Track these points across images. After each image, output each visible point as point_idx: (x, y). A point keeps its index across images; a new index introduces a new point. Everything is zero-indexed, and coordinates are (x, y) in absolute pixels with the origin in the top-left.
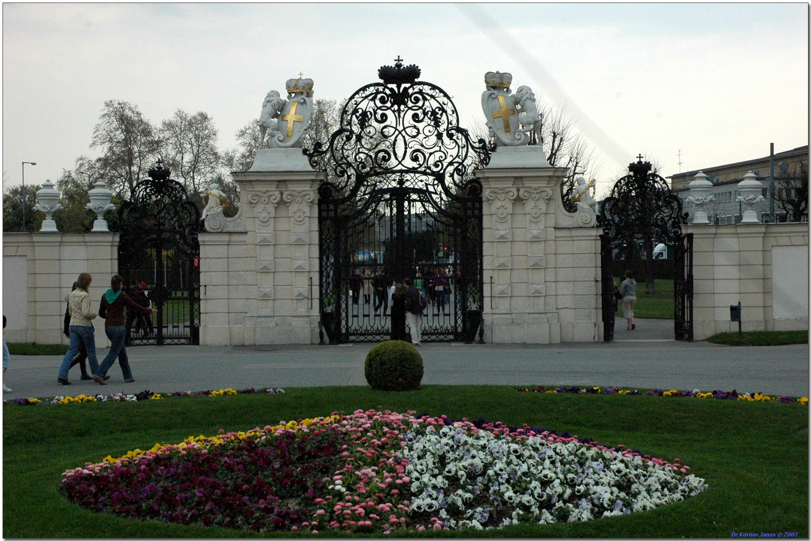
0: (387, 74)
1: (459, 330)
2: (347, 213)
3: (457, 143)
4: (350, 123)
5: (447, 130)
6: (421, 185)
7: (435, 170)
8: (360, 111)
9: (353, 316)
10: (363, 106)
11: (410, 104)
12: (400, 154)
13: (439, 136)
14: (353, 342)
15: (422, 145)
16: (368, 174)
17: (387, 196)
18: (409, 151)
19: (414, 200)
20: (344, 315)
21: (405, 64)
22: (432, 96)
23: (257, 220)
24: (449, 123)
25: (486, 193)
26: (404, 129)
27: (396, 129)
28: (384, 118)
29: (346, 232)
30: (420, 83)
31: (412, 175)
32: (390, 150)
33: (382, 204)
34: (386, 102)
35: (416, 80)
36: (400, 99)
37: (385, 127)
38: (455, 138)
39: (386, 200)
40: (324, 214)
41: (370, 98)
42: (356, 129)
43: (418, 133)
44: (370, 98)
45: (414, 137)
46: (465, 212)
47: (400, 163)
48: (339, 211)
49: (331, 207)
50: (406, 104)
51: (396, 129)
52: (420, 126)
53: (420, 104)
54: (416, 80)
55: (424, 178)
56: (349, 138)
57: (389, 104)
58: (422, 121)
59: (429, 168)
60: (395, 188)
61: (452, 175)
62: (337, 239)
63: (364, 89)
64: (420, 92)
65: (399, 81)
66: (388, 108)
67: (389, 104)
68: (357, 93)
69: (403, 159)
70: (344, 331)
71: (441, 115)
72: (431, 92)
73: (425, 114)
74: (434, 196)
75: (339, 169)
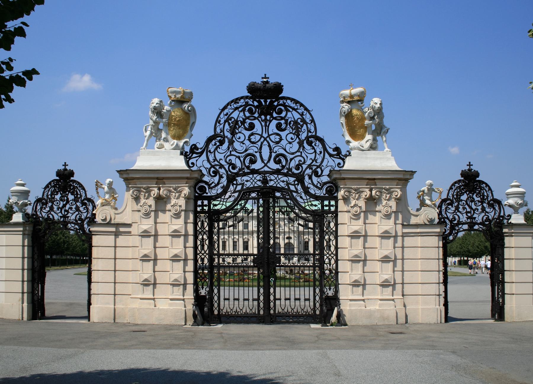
0: (254, 90)
1: (318, 312)
3: (314, 148)
4: (222, 131)
5: (307, 138)
6: (283, 185)
7: (296, 172)
8: (233, 120)
9: (225, 299)
10: (235, 115)
11: (275, 115)
12: (266, 156)
13: (301, 144)
15: (285, 150)
16: (237, 174)
17: (254, 195)
18: (274, 155)
19: (279, 198)
20: (216, 298)
21: (272, 80)
24: (309, 131)
25: (341, 193)
26: (269, 136)
27: (262, 136)
29: (218, 225)
30: (283, 98)
31: (276, 176)
32: (257, 155)
33: (250, 201)
34: (254, 113)
35: (280, 96)
36: (266, 111)
38: (313, 144)
39: (253, 198)
41: (240, 109)
43: (281, 139)
44: (240, 109)
45: (277, 143)
47: (266, 165)
48: (212, 206)
49: (206, 202)
50: (271, 115)
51: (262, 136)
52: (283, 134)
54: (280, 96)
55: (285, 179)
56: (222, 143)
58: (284, 130)
59: (290, 169)
60: (260, 186)
61: (310, 177)
65: (266, 97)
66: (255, 118)
67: (256, 115)
71: (302, 126)
73: (286, 123)
74: (295, 194)
75: (212, 169)
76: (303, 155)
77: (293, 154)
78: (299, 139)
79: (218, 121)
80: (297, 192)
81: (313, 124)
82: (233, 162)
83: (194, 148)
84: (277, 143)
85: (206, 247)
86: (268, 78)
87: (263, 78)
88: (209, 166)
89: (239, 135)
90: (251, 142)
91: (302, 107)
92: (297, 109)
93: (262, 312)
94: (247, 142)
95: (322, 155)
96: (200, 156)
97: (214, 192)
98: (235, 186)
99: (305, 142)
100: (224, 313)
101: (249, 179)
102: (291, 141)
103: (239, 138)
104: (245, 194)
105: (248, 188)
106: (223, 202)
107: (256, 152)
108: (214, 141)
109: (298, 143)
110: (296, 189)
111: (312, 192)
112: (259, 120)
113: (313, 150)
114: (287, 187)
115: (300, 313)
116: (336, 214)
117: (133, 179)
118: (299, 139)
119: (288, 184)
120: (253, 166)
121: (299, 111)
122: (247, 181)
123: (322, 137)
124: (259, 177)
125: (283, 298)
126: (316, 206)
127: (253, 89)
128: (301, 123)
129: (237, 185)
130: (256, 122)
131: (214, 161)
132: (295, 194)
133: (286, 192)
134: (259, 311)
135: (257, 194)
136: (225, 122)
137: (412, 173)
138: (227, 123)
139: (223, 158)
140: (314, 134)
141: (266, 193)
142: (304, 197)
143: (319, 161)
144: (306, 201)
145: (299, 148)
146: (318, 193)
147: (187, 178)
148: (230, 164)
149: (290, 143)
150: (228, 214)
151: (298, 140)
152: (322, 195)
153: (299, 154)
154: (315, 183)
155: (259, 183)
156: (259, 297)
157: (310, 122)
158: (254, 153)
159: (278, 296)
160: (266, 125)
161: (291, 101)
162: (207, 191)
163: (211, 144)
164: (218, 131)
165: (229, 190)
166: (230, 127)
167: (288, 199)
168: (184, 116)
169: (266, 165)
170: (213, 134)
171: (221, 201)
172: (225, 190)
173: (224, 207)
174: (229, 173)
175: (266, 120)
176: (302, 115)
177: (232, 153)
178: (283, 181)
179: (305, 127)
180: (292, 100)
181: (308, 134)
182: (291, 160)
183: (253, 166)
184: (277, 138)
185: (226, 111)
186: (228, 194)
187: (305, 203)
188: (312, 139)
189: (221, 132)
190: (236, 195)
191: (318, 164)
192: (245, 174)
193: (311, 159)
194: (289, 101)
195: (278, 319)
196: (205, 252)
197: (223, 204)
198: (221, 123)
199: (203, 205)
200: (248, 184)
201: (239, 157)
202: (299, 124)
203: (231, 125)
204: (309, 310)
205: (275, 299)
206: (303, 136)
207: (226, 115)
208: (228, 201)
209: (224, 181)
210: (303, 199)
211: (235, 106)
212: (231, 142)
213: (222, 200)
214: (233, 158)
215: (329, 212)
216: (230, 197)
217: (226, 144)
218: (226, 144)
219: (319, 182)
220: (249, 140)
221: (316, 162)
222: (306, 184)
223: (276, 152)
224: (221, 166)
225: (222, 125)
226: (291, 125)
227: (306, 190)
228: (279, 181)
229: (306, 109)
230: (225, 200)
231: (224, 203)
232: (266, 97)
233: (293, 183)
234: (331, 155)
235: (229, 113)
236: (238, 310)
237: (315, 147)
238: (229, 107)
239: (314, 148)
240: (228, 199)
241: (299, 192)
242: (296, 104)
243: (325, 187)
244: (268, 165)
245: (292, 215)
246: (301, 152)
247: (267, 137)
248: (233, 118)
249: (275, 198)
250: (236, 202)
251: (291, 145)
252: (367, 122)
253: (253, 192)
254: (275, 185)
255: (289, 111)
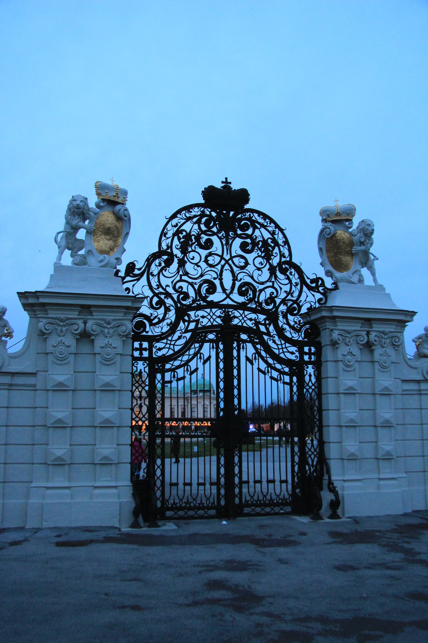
2: (164, 352)
3: (288, 278)
4: (170, 247)
5: (280, 264)
6: (250, 324)
8: (184, 233)
10: (187, 227)
11: (239, 232)
12: (228, 285)
13: (272, 270)
14: (248, 515)
15: (252, 277)
16: (190, 308)
17: (211, 336)
18: (238, 284)
19: (245, 341)
21: (235, 186)
22: (262, 226)
23: (50, 357)
24: (282, 255)
26: (232, 258)
27: (222, 257)
28: (209, 244)
29: (163, 377)
31: (241, 312)
33: (206, 346)
37: (210, 254)
38: (288, 273)
39: (210, 341)
40: (137, 354)
41: (195, 220)
42: (177, 252)
43: (247, 263)
44: (195, 220)
45: (242, 268)
46: (301, 357)
47: (228, 296)
48: (154, 350)
51: (222, 257)
52: (250, 257)
53: (250, 232)
54: (246, 207)
55: (253, 316)
56: (168, 263)
57: (215, 229)
61: (285, 316)
62: (152, 385)
63: (188, 208)
64: (250, 219)
65: (226, 206)
66: (214, 234)
68: (179, 212)
69: (231, 292)
70: (159, 504)
71: (273, 248)
72: (261, 221)
74: (266, 337)
76: (276, 285)
77: (262, 283)
78: (270, 264)
79: (163, 234)
80: (268, 334)
81: (286, 246)
82: (185, 290)
83: (131, 267)
84: (242, 268)
85: (145, 409)
86: (230, 183)
87: (223, 182)
88: (151, 295)
89: (192, 255)
90: (208, 264)
91: (272, 225)
92: (266, 226)
93: (223, 502)
94: (203, 265)
95: (299, 287)
96: (138, 280)
97: (157, 331)
98: (186, 323)
99: (277, 269)
100: (170, 506)
101: (206, 314)
102: (260, 266)
103: (193, 259)
104: (198, 335)
105: (204, 327)
106: (170, 344)
107: (215, 279)
108: (157, 262)
109: (269, 270)
110: (267, 329)
111: (288, 334)
112: (218, 236)
113: (287, 281)
114: (255, 328)
115: (275, 501)
116: (318, 365)
117: (44, 305)
118: (270, 264)
119: (257, 323)
120: (211, 298)
121: (270, 229)
122: (203, 317)
123: (299, 265)
124: (218, 313)
125: (251, 480)
126: (292, 353)
127: (210, 193)
128: (273, 245)
129: (189, 322)
130: (215, 239)
131: (158, 288)
132: (266, 337)
133: (255, 335)
134: (219, 500)
135: (216, 336)
136: (174, 235)
137: (413, 313)
138: (176, 237)
139: (170, 285)
140: (288, 259)
141: (227, 335)
142: (279, 343)
143: (296, 294)
144: (280, 347)
145: (271, 276)
146: (296, 336)
147: (127, 308)
148: (181, 293)
149: (259, 269)
150: (177, 363)
151: (268, 266)
152: (300, 339)
153: (270, 284)
154: (292, 323)
155: (219, 321)
156: (218, 479)
157: (283, 244)
158: (212, 280)
159: (245, 478)
160: (227, 243)
161: (259, 216)
162: (148, 329)
163: (153, 265)
164: (164, 247)
165: (179, 329)
166: (180, 243)
167: (257, 343)
168: (117, 223)
169: (228, 296)
170: (157, 250)
171: (167, 343)
172: (173, 327)
173: (171, 352)
174: (179, 305)
175: (227, 237)
176: (273, 234)
177: (184, 278)
178: (251, 320)
179: (276, 250)
180: (260, 213)
181: (281, 259)
182: (261, 291)
183: (211, 298)
184: (242, 262)
185: (174, 221)
186: (177, 334)
187: (279, 349)
188: (286, 266)
189: (168, 249)
190: (188, 335)
191: (294, 299)
192: (199, 308)
193: (285, 292)
194: (256, 215)
195: (247, 510)
196: (144, 416)
197: (169, 348)
198: (167, 236)
199: (141, 349)
200: (205, 322)
201: (192, 284)
202: (271, 246)
203: (182, 240)
204: (287, 496)
205: (241, 482)
206: (275, 261)
207: (175, 226)
208: (178, 343)
209: (172, 315)
210: (277, 345)
211: (188, 215)
212: (182, 263)
213: (169, 342)
214: (184, 285)
215: (310, 363)
216: (180, 338)
217: (175, 265)
218: (175, 265)
219: (296, 323)
220: (206, 261)
221: (292, 296)
222: (280, 324)
223: (241, 279)
224: (168, 295)
225: (170, 239)
226: (259, 246)
227: (280, 332)
228: (245, 319)
229: (277, 226)
230: (173, 343)
231: (172, 347)
232: (226, 206)
233: (263, 322)
234: (310, 288)
235: (179, 225)
236: (190, 500)
237: (291, 277)
238: (178, 216)
239: (288, 278)
240: (176, 340)
241: (272, 334)
242: (265, 220)
243: (304, 329)
244: (231, 296)
245: (263, 366)
246: (273, 282)
247: (229, 260)
248: (184, 230)
249: (240, 341)
250: (186, 347)
251: (260, 272)
252: (356, 249)
253: (211, 332)
254: (240, 324)
255: (257, 228)
